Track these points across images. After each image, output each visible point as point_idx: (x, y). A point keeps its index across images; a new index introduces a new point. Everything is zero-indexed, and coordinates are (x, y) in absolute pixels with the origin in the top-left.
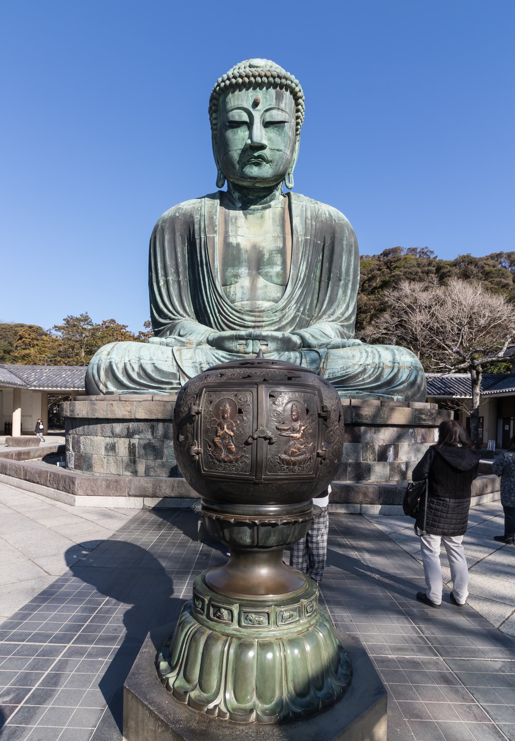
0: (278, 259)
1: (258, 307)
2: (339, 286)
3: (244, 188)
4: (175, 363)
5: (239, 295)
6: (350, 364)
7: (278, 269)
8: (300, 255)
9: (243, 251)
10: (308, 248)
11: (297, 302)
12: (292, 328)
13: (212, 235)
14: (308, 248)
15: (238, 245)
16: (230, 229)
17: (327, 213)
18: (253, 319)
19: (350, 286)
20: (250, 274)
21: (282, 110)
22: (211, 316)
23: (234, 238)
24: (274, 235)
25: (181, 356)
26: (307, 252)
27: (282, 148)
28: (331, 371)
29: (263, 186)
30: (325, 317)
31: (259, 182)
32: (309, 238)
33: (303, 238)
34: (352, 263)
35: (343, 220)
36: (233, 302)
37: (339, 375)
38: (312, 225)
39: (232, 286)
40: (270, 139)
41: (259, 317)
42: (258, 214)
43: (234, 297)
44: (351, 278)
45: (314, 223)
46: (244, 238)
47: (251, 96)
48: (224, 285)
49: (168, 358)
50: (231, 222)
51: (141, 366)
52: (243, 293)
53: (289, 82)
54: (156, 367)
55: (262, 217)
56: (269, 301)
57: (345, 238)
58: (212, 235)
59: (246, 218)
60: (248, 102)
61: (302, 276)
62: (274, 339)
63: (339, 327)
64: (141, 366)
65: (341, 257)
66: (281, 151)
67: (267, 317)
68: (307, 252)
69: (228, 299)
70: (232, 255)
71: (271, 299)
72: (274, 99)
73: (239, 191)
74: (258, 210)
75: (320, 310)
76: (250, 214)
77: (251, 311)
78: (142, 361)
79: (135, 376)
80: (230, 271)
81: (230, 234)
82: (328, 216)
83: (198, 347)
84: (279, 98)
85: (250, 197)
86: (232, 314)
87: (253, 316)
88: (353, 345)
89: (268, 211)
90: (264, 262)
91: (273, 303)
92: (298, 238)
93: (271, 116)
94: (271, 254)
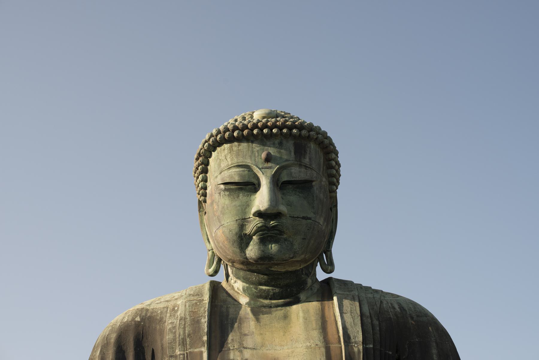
13: (197, 350)
17: (397, 307)
21: (306, 167)
23: (237, 353)
24: (309, 344)
27: (311, 215)
29: (283, 270)
31: (277, 264)
32: (371, 346)
33: (361, 347)
38: (373, 325)
40: (289, 204)
42: (280, 312)
45: (376, 322)
46: (255, 351)
47: (258, 151)
55: (286, 317)
57: (434, 344)
58: (197, 350)
59: (258, 320)
60: (253, 158)
66: (310, 219)
72: (293, 153)
74: (277, 306)
76: (264, 313)
81: (229, 345)
82: (398, 309)
84: (300, 151)
89: (295, 307)
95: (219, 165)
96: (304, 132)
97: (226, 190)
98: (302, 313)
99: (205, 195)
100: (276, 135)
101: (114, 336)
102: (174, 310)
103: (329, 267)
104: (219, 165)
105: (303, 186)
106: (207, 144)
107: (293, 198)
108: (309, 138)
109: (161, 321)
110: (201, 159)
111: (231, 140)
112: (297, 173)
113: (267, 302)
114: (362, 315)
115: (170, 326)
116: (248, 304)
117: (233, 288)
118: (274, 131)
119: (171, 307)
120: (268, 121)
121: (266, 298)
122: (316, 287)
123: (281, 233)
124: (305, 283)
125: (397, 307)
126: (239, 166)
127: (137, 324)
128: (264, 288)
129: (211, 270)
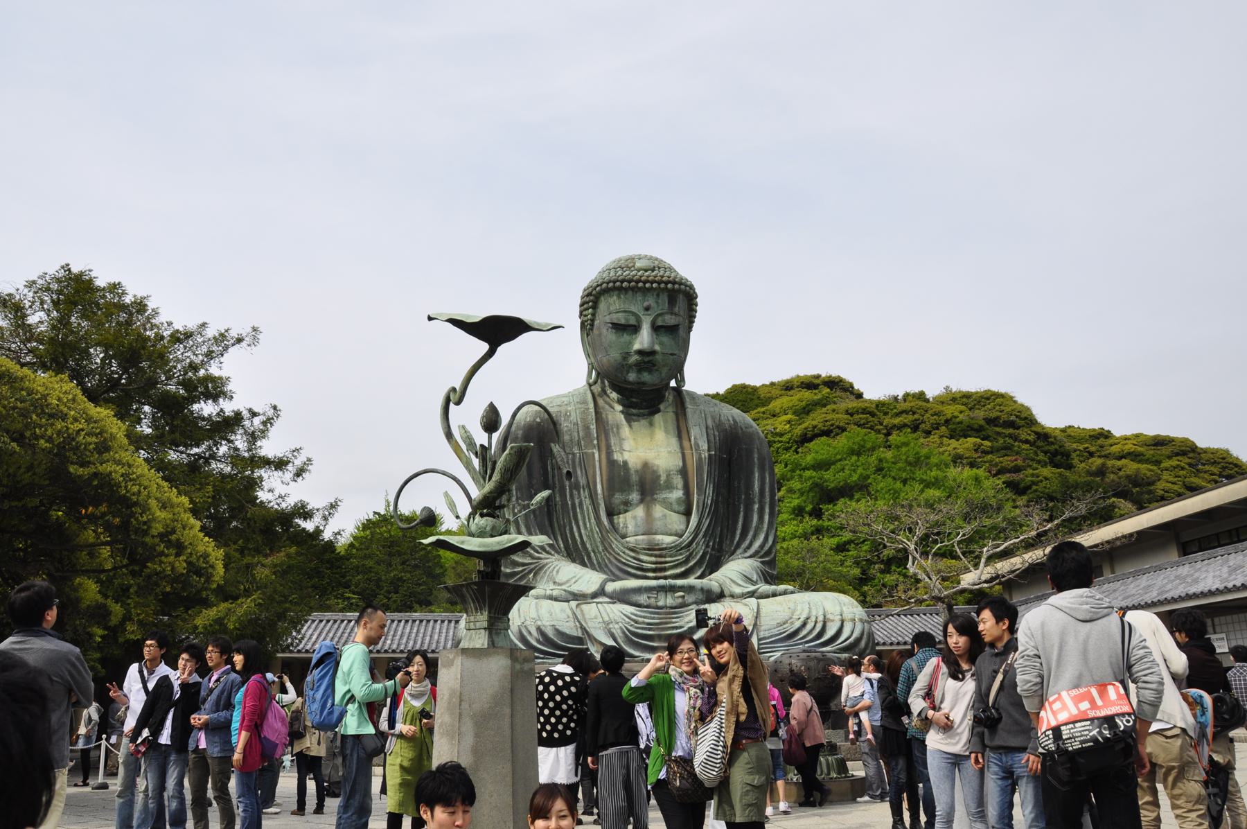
0: (678, 481)
5: (631, 528)
7: (678, 494)
9: (632, 472)
11: (704, 536)
15: (625, 463)
18: (653, 559)
19: (767, 510)
25: (583, 615)
30: (739, 551)
36: (624, 537)
37: (775, 631)
40: (661, 344)
41: (660, 556)
43: (624, 531)
44: (767, 499)
48: (610, 514)
51: (539, 629)
54: (557, 630)
55: (651, 424)
64: (539, 629)
65: (753, 473)
70: (619, 477)
78: (539, 623)
79: (535, 643)
80: (618, 498)
84: (672, 301)
87: (651, 555)
88: (785, 593)
89: (657, 416)
93: (664, 321)
94: (668, 476)
96: (676, 286)
99: (592, 325)
102: (567, 416)
103: (681, 381)
107: (665, 339)
108: (679, 291)
111: (620, 289)
112: (670, 320)
113: (635, 411)
114: (707, 428)
116: (622, 412)
122: (671, 398)
127: (539, 424)
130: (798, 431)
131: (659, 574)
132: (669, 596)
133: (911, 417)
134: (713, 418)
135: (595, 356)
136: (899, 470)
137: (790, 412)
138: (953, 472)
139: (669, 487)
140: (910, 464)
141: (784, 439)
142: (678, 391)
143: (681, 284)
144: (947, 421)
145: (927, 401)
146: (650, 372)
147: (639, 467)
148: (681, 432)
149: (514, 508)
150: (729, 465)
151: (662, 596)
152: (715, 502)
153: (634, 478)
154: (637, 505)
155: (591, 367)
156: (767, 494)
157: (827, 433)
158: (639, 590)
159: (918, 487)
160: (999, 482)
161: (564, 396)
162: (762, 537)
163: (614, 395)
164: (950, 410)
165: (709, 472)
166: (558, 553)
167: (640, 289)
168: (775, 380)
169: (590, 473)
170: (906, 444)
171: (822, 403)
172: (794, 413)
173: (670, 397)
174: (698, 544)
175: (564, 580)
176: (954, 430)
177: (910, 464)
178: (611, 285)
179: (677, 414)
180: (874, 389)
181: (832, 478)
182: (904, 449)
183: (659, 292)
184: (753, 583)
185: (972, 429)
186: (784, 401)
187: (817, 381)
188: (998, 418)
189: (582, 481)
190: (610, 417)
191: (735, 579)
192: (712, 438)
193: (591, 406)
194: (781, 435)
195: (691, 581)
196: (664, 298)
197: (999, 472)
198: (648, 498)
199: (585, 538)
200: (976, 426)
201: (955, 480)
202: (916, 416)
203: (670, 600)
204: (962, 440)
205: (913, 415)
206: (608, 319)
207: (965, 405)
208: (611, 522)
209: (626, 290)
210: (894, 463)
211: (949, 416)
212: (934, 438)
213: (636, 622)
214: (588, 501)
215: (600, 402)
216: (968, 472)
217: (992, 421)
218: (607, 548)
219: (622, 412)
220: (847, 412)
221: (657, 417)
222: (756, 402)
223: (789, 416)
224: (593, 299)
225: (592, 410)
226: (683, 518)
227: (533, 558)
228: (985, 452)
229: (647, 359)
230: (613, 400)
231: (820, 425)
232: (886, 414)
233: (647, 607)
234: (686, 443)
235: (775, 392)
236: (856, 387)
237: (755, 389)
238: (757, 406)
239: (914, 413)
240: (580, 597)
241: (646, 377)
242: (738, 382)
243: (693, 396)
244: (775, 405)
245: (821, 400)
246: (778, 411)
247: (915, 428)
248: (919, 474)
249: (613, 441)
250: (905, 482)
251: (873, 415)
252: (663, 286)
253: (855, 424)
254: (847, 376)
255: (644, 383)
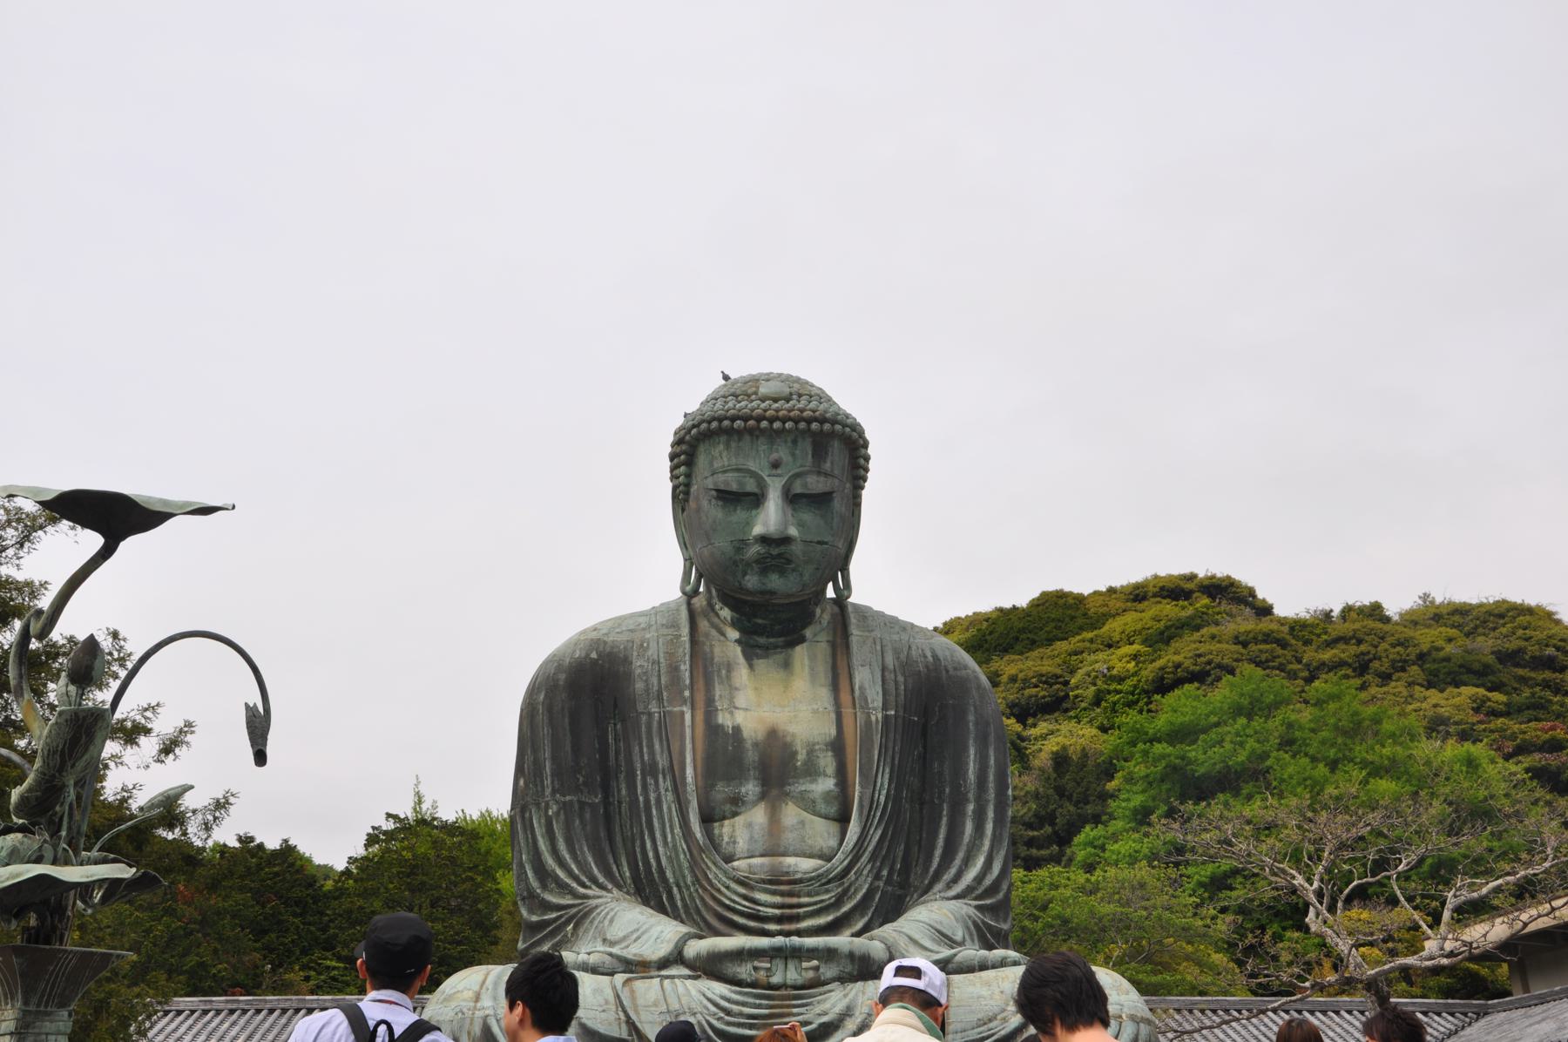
0: (827, 762)
1: (788, 873)
2: (964, 814)
3: (745, 602)
4: (622, 1015)
5: (742, 845)
6: (996, 1010)
7: (827, 784)
8: (876, 753)
9: (748, 745)
10: (891, 735)
11: (873, 858)
12: (866, 919)
14: (891, 735)
15: (737, 729)
16: (717, 693)
17: (929, 654)
18: (778, 899)
19: (991, 814)
20: (763, 796)
21: (826, 475)
22: (675, 890)
23: (728, 716)
26: (891, 745)
28: (959, 1026)
30: (939, 886)
34: (992, 762)
35: (966, 667)
36: (729, 859)
38: (896, 682)
39: (726, 822)
40: (801, 525)
41: (791, 894)
42: (780, 657)
43: (730, 849)
44: (991, 794)
45: (901, 679)
48: (708, 819)
49: (607, 1002)
50: (719, 676)
52: (751, 838)
53: (838, 427)
55: (787, 665)
56: (811, 856)
59: (751, 667)
61: (882, 799)
62: (830, 954)
63: (972, 911)
65: (965, 749)
67: (809, 895)
68: (891, 745)
69: (718, 852)
70: (726, 755)
71: (816, 851)
73: (732, 608)
74: (776, 647)
75: (926, 869)
77: (771, 882)
80: (722, 790)
81: (718, 704)
83: (664, 973)
84: (820, 451)
85: (760, 621)
86: (728, 888)
87: (774, 893)
89: (798, 649)
90: (796, 768)
91: (820, 862)
92: (868, 715)
93: (805, 485)
94: (810, 752)
95: (711, 464)
96: (827, 426)
97: (718, 498)
98: (807, 658)
99: (687, 493)
100: (790, 431)
101: (562, 677)
104: (711, 464)
105: (820, 501)
106: (694, 431)
107: (807, 516)
108: (832, 434)
109: (627, 661)
110: (684, 447)
111: (730, 432)
112: (816, 484)
113: (762, 640)
114: (884, 669)
115: (638, 671)
116: (738, 641)
117: (717, 615)
118: (789, 425)
119: (637, 642)
120: (777, 411)
121: (761, 635)
122: (826, 618)
123: (789, 561)
124: (812, 614)
125: (929, 654)
126: (738, 470)
127: (594, 662)
128: (760, 621)
129: (688, 588)
130: (1149, 672)
131: (786, 927)
132: (791, 966)
133: (1353, 649)
134: (897, 652)
135: (693, 548)
136: (1323, 742)
137: (1138, 639)
138: (1426, 748)
139: (811, 771)
140: (1345, 733)
141: (1126, 686)
142: (841, 602)
143: (834, 422)
144: (1421, 657)
145: (1387, 620)
146: (782, 572)
147: (760, 736)
148: (838, 676)
149: (547, 807)
150: (924, 734)
151: (779, 963)
152: (894, 798)
153: (751, 756)
154: (755, 803)
155: (689, 562)
156: (991, 785)
157: (1199, 677)
158: (740, 955)
159: (1358, 774)
160: (1516, 768)
161: (642, 614)
162: (980, 862)
163: (726, 613)
164: (1426, 638)
165: (883, 748)
166: (619, 887)
167: (763, 431)
168: (1118, 582)
169: (675, 748)
170: (1336, 697)
171: (1193, 624)
172: (1144, 642)
173: (824, 616)
174: (859, 874)
175: (621, 934)
176: (1435, 673)
177: (1345, 733)
178: (714, 424)
179: (833, 645)
180: (1291, 599)
181: (1204, 757)
182: (1332, 706)
183: (795, 437)
184: (951, 942)
185: (1470, 671)
186: (1129, 620)
187: (1189, 586)
188: (1520, 651)
189: (662, 762)
190: (717, 650)
191: (917, 937)
192: (891, 686)
193: (685, 631)
194: (1121, 680)
195: (842, 941)
196: (806, 446)
197: (1522, 750)
198: (775, 792)
199: (664, 861)
200: (1476, 666)
201: (1428, 763)
202: (1363, 648)
203: (793, 974)
204: (1450, 690)
205: (1362, 645)
206: (710, 483)
207: (1458, 627)
208: (709, 834)
209: (740, 433)
210: (1313, 731)
211: (1425, 648)
212: (1397, 686)
213: (728, 1012)
214: (670, 796)
215: (703, 625)
216: (1452, 750)
217: (1509, 658)
218: (700, 878)
219: (738, 641)
220: (1237, 640)
221: (800, 653)
222: (1080, 621)
223: (1136, 647)
224: (691, 446)
225: (685, 638)
226: (834, 828)
227: (575, 895)
228: (1495, 714)
229: (775, 552)
230: (724, 621)
231: (1187, 663)
232: (1307, 643)
233: (753, 985)
234: (845, 697)
235: (1116, 604)
236: (1260, 595)
237: (1080, 599)
238: (1081, 629)
239: (1360, 642)
240: (636, 968)
241: (775, 581)
242: (1051, 587)
243: (864, 613)
244: (1113, 627)
245: (1191, 618)
246: (1116, 637)
247: (1362, 668)
248: (1360, 751)
249: (718, 691)
250: (1333, 765)
251: (1283, 644)
252: (802, 425)
253: (1251, 661)
254: (1244, 575)
255: (772, 593)
